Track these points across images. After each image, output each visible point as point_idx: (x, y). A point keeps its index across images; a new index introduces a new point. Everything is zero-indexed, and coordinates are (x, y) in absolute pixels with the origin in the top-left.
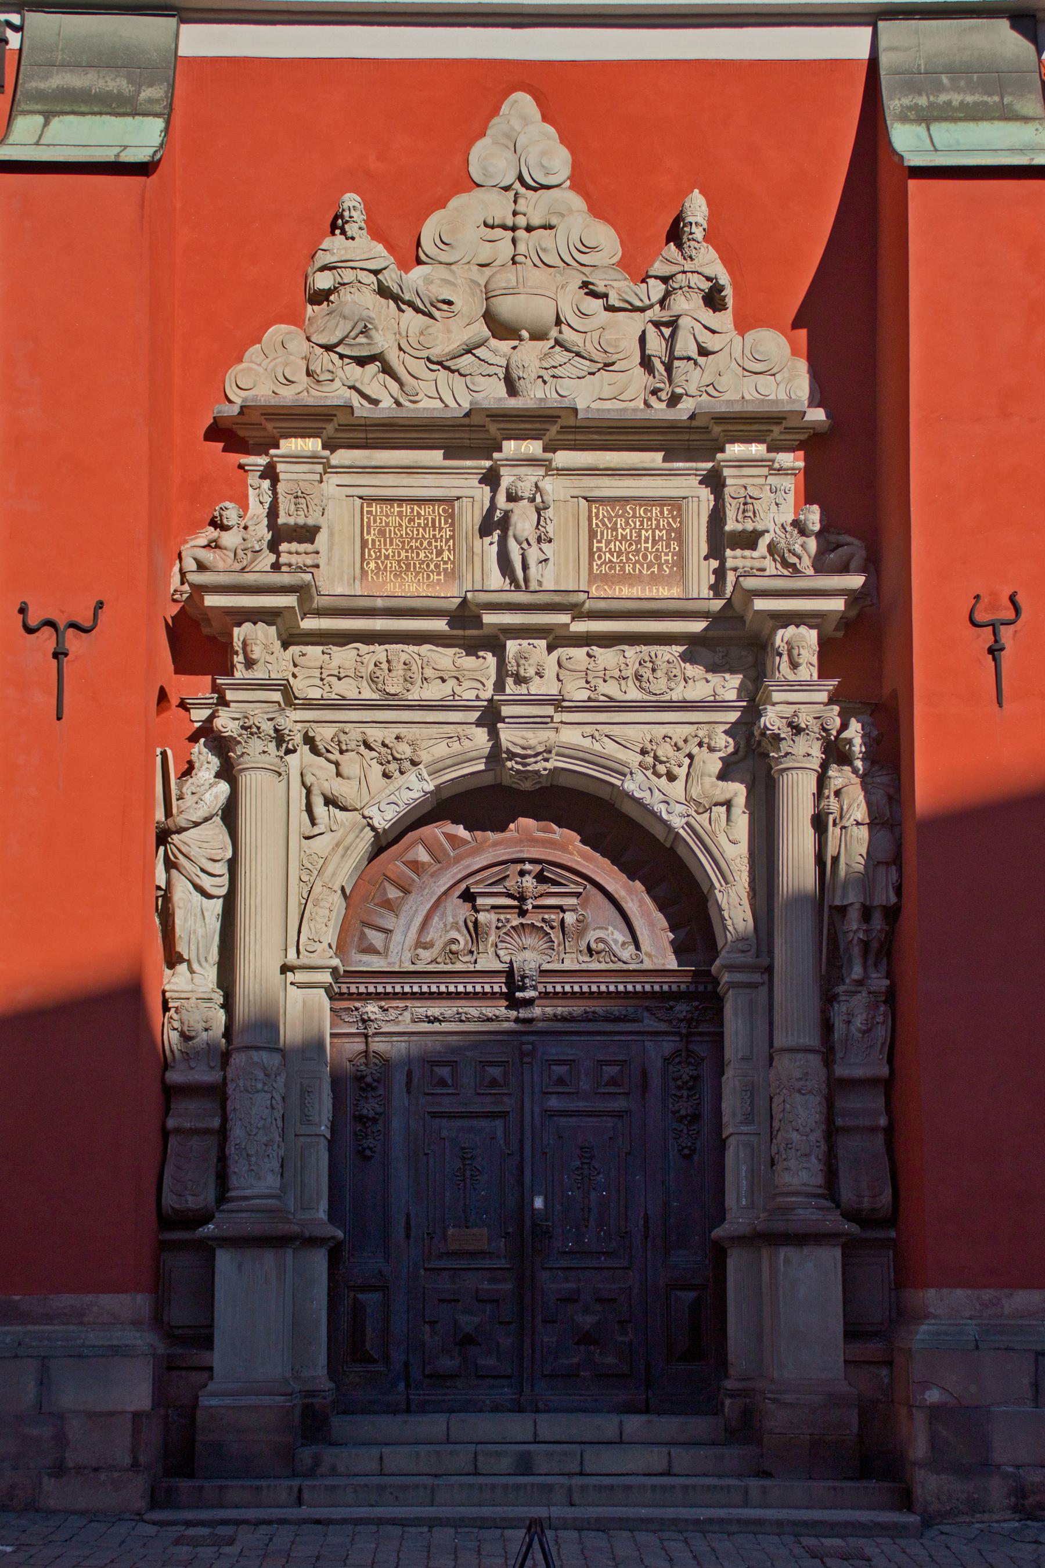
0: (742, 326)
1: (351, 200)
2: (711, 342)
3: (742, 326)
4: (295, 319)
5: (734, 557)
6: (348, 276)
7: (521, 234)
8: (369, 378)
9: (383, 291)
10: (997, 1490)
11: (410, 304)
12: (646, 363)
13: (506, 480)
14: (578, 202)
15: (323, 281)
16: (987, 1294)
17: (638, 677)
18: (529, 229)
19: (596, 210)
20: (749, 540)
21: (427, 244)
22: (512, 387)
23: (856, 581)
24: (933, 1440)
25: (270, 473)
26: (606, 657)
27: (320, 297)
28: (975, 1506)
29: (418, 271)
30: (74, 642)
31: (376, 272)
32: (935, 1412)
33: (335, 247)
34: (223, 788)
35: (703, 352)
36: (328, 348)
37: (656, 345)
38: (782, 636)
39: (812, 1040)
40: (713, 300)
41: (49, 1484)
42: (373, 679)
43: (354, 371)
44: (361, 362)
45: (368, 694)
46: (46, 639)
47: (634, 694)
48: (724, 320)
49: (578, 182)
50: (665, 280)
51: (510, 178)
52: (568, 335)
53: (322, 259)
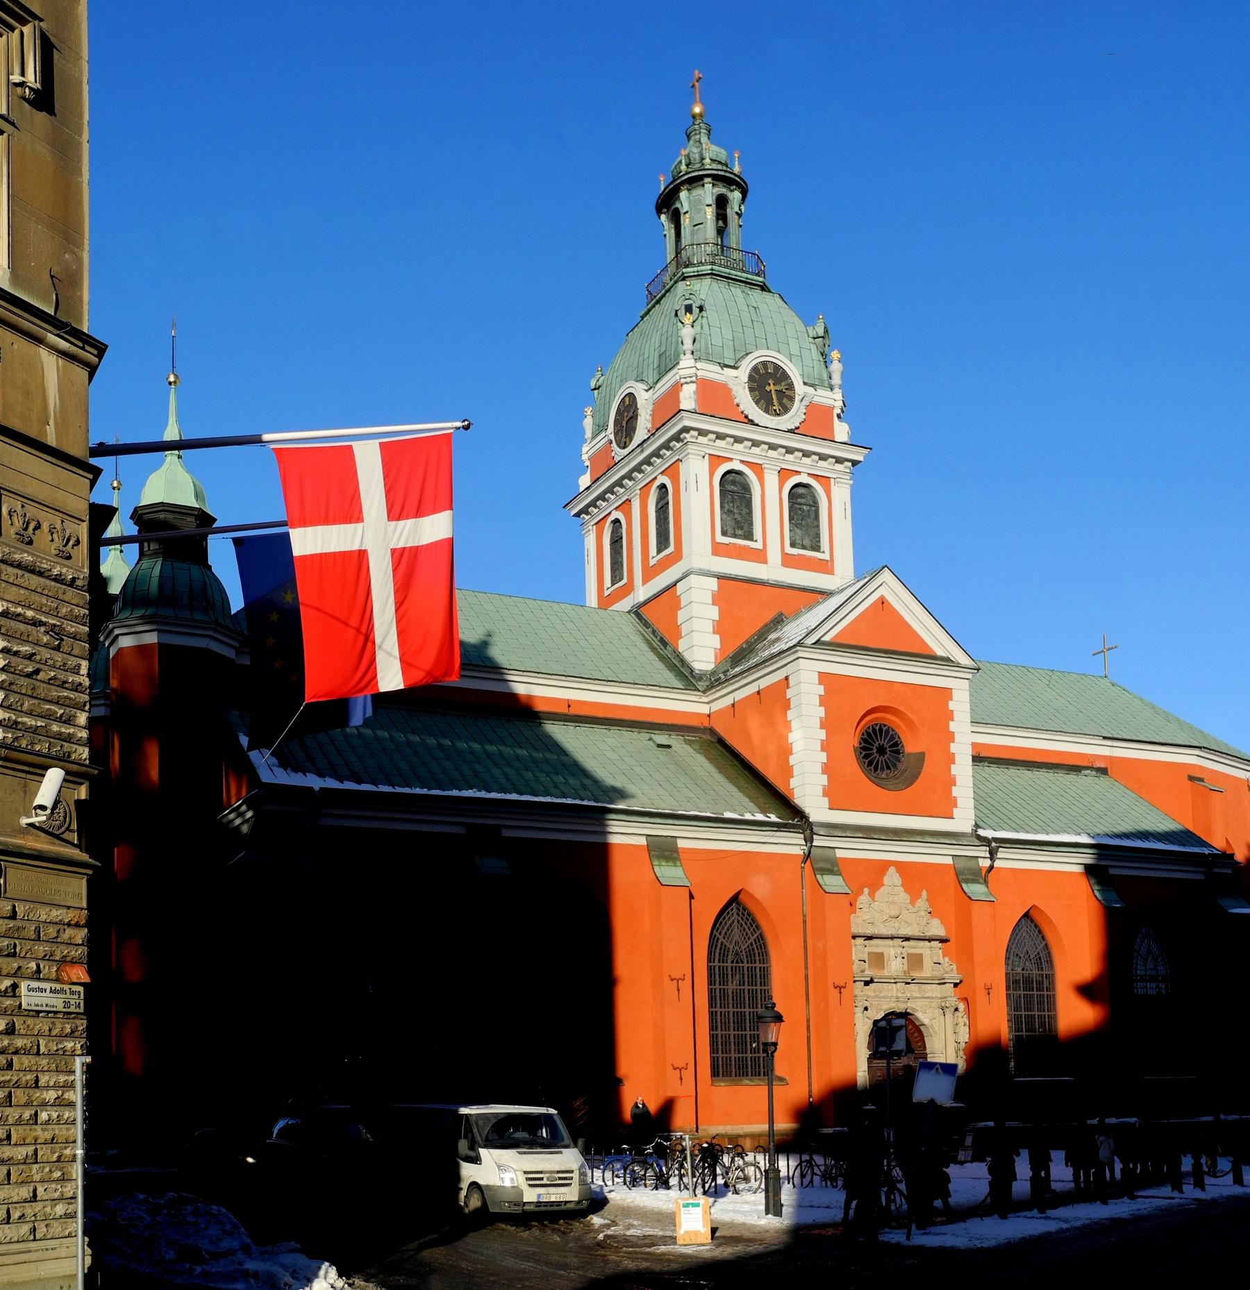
47: (918, 996)
49: (902, 885)
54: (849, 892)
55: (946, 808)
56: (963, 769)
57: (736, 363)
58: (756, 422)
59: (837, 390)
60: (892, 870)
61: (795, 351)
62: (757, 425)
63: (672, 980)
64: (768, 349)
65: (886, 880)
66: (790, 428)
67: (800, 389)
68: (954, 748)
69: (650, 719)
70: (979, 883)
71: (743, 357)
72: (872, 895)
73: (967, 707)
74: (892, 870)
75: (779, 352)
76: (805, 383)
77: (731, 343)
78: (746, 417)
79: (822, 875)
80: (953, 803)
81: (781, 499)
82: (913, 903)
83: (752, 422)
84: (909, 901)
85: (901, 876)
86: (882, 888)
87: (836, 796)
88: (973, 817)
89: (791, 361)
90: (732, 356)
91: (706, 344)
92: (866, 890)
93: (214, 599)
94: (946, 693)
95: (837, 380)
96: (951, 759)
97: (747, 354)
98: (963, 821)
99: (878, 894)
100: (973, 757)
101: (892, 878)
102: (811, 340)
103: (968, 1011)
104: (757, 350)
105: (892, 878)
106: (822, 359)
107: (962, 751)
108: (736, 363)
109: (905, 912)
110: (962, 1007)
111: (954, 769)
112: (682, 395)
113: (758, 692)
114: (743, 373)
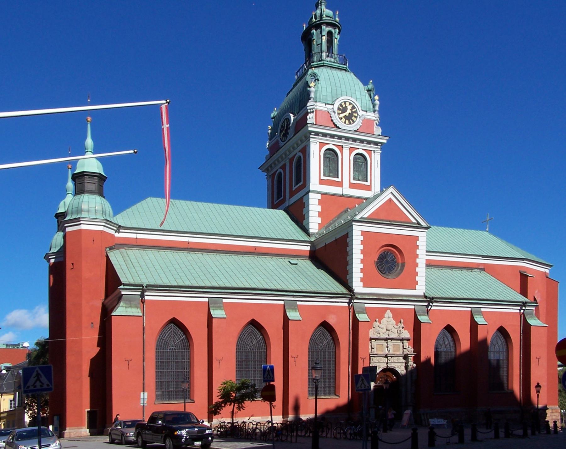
0: (404, 330)
1: (377, 319)
5: (404, 350)
8: (378, 335)
12: (398, 333)
13: (388, 343)
14: (392, 319)
15: (375, 326)
19: (394, 320)
20: (406, 349)
21: (382, 323)
22: (388, 335)
23: (416, 354)
25: (371, 343)
26: (395, 358)
27: (374, 327)
29: (381, 325)
33: (375, 323)
37: (399, 332)
38: (409, 358)
40: (403, 328)
42: (378, 360)
43: (377, 334)
45: (377, 362)
48: (403, 329)
49: (393, 317)
54: (369, 320)
55: (413, 285)
56: (421, 269)
57: (333, 102)
58: (340, 127)
59: (376, 112)
61: (358, 96)
62: (341, 129)
63: (292, 358)
64: (347, 96)
65: (386, 315)
66: (355, 129)
67: (361, 113)
68: (418, 261)
69: (289, 253)
70: (425, 316)
71: (336, 100)
73: (425, 244)
74: (389, 310)
75: (352, 97)
76: (362, 110)
77: (331, 94)
79: (358, 314)
80: (417, 283)
81: (350, 160)
83: (338, 127)
84: (395, 324)
86: (384, 319)
88: (425, 289)
89: (357, 101)
90: (331, 99)
91: (320, 94)
93: (105, 210)
94: (417, 238)
95: (377, 108)
96: (417, 265)
97: (337, 99)
98: (420, 290)
99: (382, 321)
100: (426, 265)
101: (389, 314)
102: (366, 92)
104: (342, 96)
105: (389, 314)
106: (370, 100)
107: (422, 260)
108: (333, 102)
111: (418, 270)
112: (308, 117)
113: (336, 240)
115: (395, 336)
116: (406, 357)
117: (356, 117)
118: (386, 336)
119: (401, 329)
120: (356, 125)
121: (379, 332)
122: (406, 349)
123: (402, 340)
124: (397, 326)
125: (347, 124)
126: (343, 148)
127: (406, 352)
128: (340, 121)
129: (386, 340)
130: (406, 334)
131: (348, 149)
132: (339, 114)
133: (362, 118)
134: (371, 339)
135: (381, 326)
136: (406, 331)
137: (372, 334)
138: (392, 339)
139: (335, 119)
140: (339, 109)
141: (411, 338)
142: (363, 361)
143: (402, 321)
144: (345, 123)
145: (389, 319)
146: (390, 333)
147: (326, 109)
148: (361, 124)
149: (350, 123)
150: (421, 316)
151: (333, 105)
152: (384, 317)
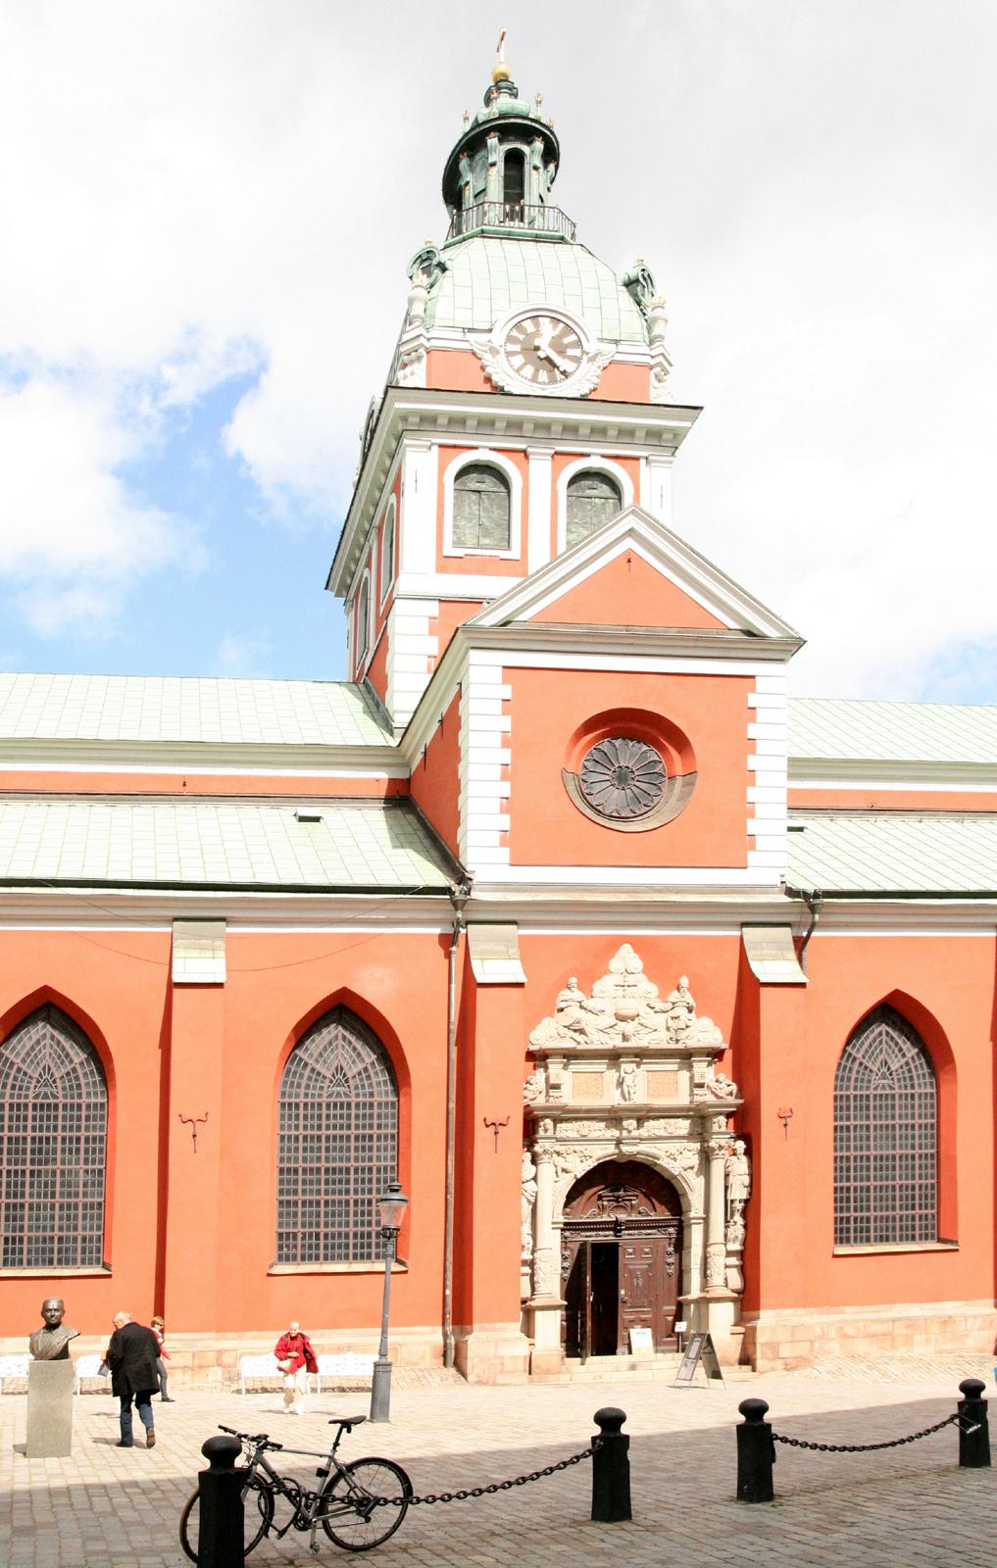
0: (698, 1016)
1: (573, 980)
2: (689, 1023)
3: (698, 1016)
4: (552, 1015)
5: (697, 1091)
6: (572, 1003)
7: (626, 988)
9: (581, 1007)
10: (779, 1364)
11: (590, 1011)
12: (668, 1029)
14: (644, 977)
15: (563, 1005)
16: (778, 1311)
17: (665, 1128)
18: (629, 986)
19: (651, 979)
20: (701, 1086)
24: (762, 1352)
28: (773, 1369)
30: (500, 1128)
31: (580, 1002)
32: (763, 1344)
33: (565, 994)
34: (534, 1167)
35: (687, 1027)
36: (565, 1027)
39: (722, 1241)
41: (499, 1376)
44: (575, 1031)
46: (493, 1128)
48: (693, 1016)
49: (644, 971)
50: (674, 1003)
51: (623, 970)
52: (643, 1021)
53: (562, 998)
60: (626, 949)
65: (615, 964)
72: (586, 988)
74: (626, 949)
78: (502, 389)
82: (663, 997)
85: (643, 957)
87: (522, 847)
92: (573, 980)
99: (597, 987)
101: (627, 958)
103: (748, 1152)
105: (627, 958)
109: (643, 1010)
110: (741, 1145)
114: (498, 338)
115: (659, 1040)
116: (700, 1119)
117: (577, 360)
118: (614, 1042)
119: (682, 1012)
120: (579, 381)
121: (583, 1025)
122: (701, 1086)
123: (686, 1056)
124: (665, 1001)
125: (544, 383)
126: (526, 456)
127: (704, 1097)
128: (516, 375)
129: (614, 1057)
130: (710, 1033)
131: (549, 458)
132: (509, 354)
133: (602, 362)
134: (538, 1058)
135: (590, 1003)
136: (706, 1022)
137: (546, 1035)
138: (641, 1055)
139: (498, 370)
140: (510, 339)
141: (725, 1046)
142: (496, 1133)
143: (684, 981)
144: (534, 379)
145: (631, 980)
146: (629, 1027)
147: (466, 346)
148: (597, 381)
149: (553, 381)
150: (764, 962)
151: (490, 330)
152: (608, 972)
